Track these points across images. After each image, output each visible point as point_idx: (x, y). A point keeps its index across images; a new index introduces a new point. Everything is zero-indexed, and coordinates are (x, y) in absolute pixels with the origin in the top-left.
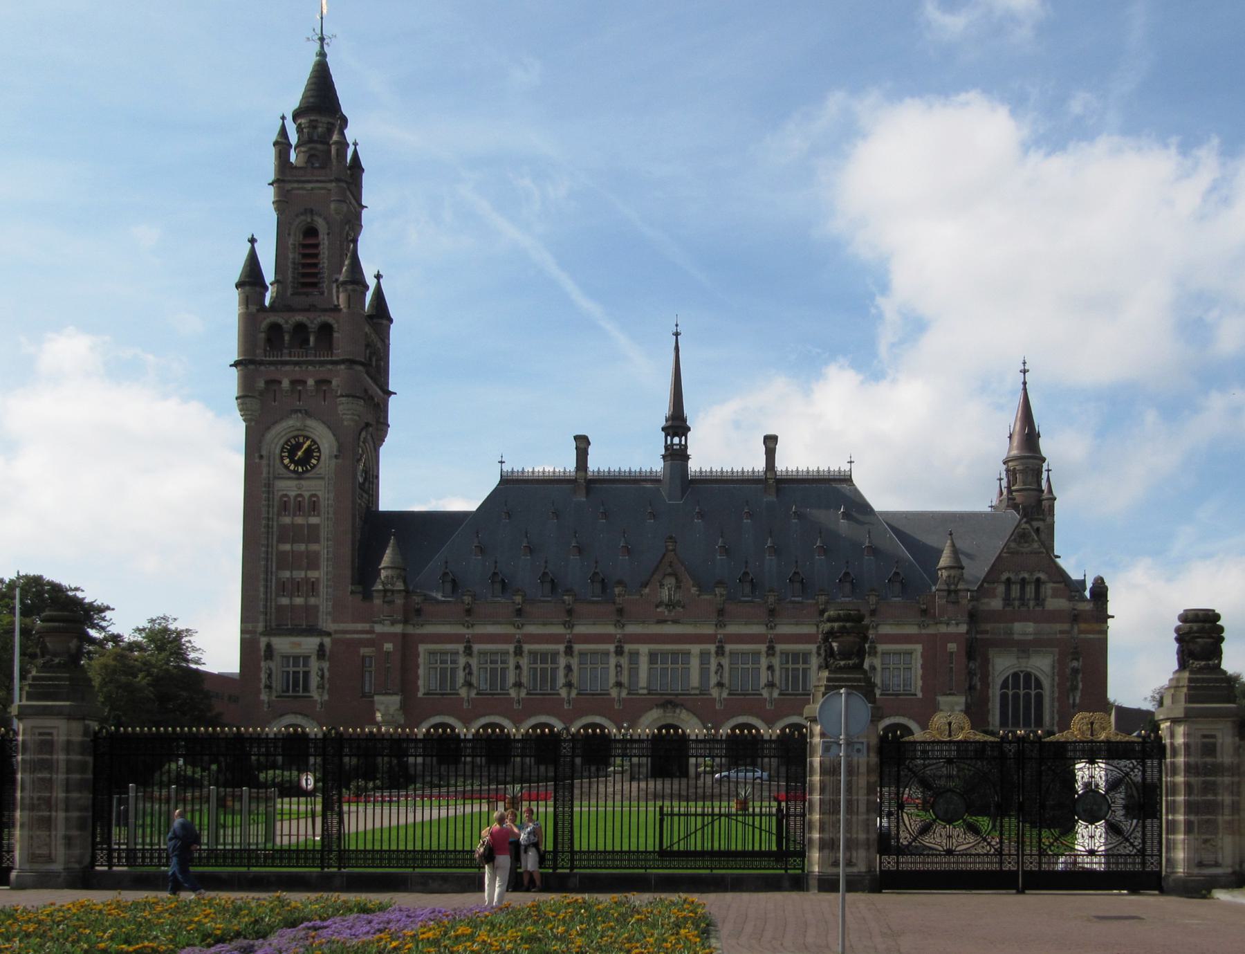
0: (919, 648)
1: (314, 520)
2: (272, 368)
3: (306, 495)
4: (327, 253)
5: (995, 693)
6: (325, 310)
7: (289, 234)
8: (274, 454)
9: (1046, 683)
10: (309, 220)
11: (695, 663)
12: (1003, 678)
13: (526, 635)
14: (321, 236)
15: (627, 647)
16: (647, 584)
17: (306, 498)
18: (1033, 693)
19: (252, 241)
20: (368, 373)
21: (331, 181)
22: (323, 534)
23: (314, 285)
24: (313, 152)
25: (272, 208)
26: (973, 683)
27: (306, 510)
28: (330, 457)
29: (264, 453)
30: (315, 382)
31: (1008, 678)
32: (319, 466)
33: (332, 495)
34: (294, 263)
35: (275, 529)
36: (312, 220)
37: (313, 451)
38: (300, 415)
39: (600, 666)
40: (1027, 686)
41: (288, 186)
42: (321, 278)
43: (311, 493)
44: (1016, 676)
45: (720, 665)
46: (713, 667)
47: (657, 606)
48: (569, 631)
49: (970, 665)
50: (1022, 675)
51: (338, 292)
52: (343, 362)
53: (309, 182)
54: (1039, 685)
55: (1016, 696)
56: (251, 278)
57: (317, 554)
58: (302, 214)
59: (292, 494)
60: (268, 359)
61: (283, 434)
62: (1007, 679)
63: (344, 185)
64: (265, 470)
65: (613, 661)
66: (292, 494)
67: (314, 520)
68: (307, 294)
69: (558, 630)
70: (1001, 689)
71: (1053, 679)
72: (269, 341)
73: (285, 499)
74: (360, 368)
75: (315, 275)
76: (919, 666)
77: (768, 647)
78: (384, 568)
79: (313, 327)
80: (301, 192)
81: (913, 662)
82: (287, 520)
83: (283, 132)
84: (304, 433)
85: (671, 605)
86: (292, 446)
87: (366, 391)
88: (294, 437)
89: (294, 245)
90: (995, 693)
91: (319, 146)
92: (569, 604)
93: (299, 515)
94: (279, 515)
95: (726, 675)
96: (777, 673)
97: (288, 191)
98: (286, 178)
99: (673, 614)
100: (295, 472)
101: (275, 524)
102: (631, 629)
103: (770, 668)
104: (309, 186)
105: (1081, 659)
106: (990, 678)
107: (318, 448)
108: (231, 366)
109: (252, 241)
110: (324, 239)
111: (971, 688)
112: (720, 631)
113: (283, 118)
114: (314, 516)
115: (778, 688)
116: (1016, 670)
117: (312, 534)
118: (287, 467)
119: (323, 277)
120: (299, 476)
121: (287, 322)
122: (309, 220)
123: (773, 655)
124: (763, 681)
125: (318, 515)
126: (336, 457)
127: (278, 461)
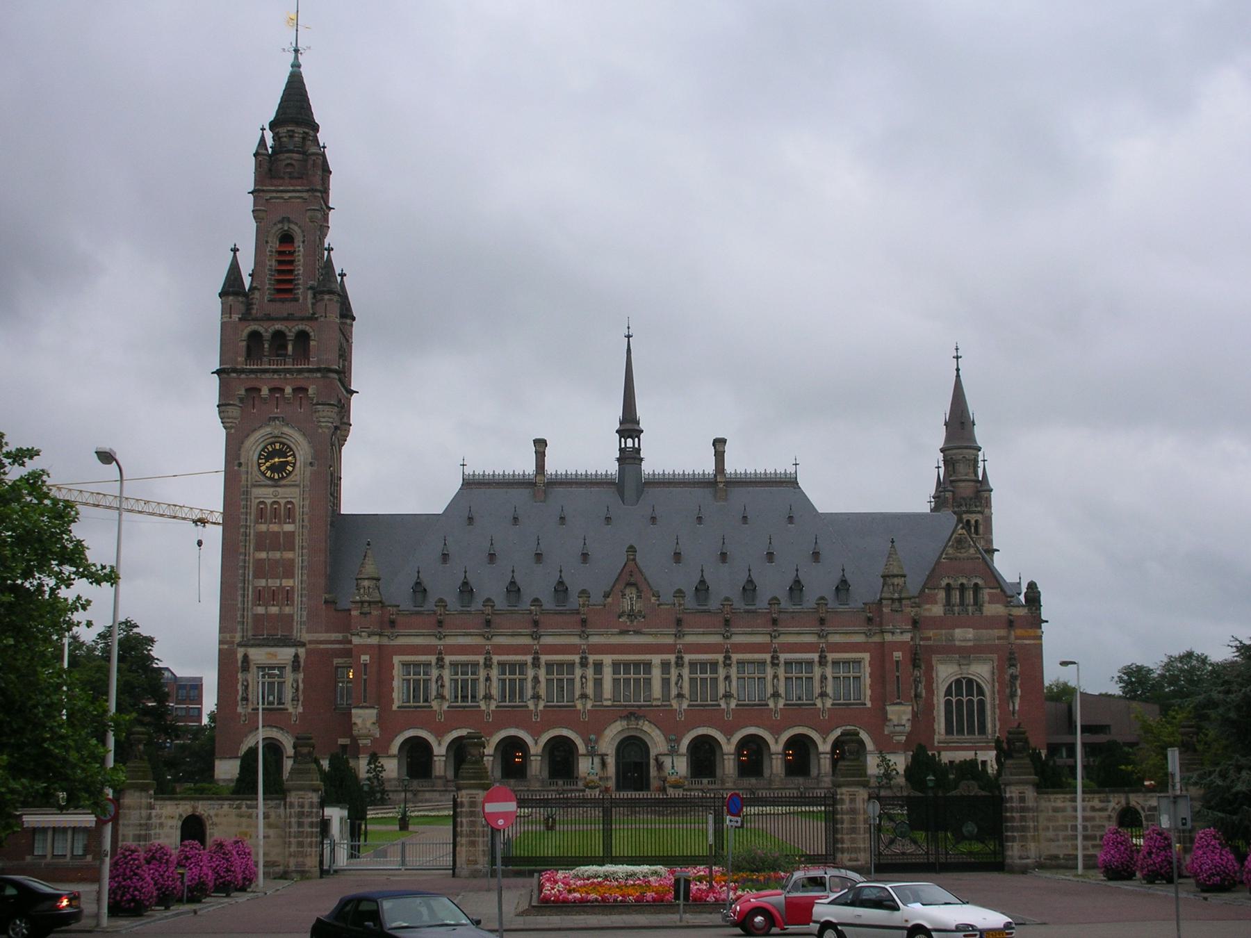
0: (866, 656)
1: (288, 528)
2: (253, 376)
3: (282, 501)
4: (301, 258)
6: (302, 319)
7: (267, 242)
8: (252, 459)
10: (286, 228)
11: (656, 673)
12: (947, 685)
13: (495, 646)
15: (591, 658)
16: (610, 594)
17: (282, 505)
18: (975, 699)
19: (235, 250)
20: (340, 380)
24: (289, 161)
26: (919, 690)
27: (283, 519)
29: (242, 461)
30: (293, 390)
31: (951, 684)
33: (307, 503)
34: (271, 270)
35: (252, 537)
38: (277, 422)
39: (565, 676)
40: (970, 693)
41: (268, 196)
42: (296, 285)
43: (286, 500)
44: (958, 682)
45: (680, 676)
46: (674, 679)
47: (620, 617)
48: (536, 642)
49: (915, 672)
52: (318, 370)
54: (981, 692)
55: (959, 703)
56: (232, 287)
57: (293, 560)
58: (279, 222)
59: (269, 501)
60: (248, 367)
61: (262, 440)
63: (319, 194)
65: (578, 672)
66: (269, 501)
67: (288, 528)
68: (283, 301)
69: (527, 641)
70: (945, 696)
71: (994, 686)
72: (248, 347)
73: (262, 506)
74: (335, 376)
75: (290, 281)
77: (725, 657)
79: (291, 335)
80: (278, 201)
81: (862, 670)
82: (263, 528)
83: (263, 140)
84: (281, 440)
85: (631, 615)
86: (269, 453)
88: (273, 443)
89: (271, 251)
91: (296, 156)
92: (536, 615)
93: (275, 523)
94: (257, 522)
95: (686, 685)
96: (734, 683)
97: (267, 200)
98: (265, 188)
99: (635, 623)
100: (271, 479)
101: (252, 531)
102: (594, 640)
103: (727, 678)
104: (287, 195)
105: (1019, 666)
106: (935, 685)
108: (213, 373)
109: (235, 250)
110: (300, 247)
113: (263, 129)
114: (289, 523)
115: (735, 698)
116: (959, 676)
117: (288, 542)
118: (264, 474)
119: (298, 284)
120: (276, 483)
121: (266, 331)
123: (730, 665)
124: (721, 691)
125: (294, 522)
126: (311, 463)
127: (256, 468)
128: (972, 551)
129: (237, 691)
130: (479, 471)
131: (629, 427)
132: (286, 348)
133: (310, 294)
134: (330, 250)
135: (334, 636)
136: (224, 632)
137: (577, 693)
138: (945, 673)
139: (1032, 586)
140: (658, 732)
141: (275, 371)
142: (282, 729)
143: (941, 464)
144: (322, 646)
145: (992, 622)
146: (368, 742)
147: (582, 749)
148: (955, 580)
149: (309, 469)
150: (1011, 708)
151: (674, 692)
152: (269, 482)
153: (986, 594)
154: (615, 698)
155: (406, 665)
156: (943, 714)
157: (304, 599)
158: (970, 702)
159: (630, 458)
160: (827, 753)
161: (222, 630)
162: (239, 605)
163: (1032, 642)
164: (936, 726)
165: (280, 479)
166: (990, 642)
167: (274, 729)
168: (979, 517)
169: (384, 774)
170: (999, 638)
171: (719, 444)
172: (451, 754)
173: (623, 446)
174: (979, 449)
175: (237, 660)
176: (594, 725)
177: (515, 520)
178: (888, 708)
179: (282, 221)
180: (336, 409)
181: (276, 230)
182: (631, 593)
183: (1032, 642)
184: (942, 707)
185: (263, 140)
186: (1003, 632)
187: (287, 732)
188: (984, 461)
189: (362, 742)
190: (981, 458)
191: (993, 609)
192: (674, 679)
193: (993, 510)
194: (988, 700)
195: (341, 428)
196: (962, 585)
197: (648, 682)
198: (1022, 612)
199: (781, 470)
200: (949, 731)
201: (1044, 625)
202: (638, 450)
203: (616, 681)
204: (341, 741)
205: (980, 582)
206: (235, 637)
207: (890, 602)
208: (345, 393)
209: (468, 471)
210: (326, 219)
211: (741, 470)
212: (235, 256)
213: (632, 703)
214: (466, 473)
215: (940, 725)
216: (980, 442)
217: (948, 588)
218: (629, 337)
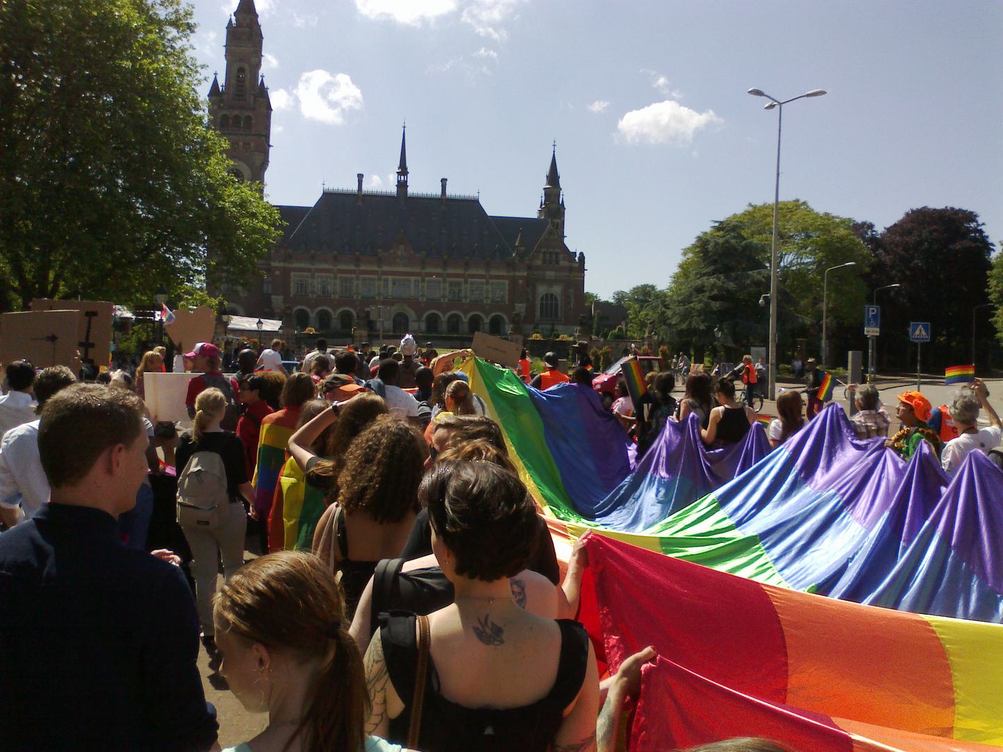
5: (538, 302)
9: (559, 298)
11: (412, 285)
12: (542, 295)
15: (384, 277)
18: (554, 302)
19: (216, 74)
25: (224, 58)
30: (244, 144)
40: (551, 300)
44: (547, 295)
54: (556, 299)
55: (547, 303)
62: (542, 298)
83: (230, 21)
90: (538, 302)
102: (385, 268)
104: (242, 48)
109: (216, 74)
110: (248, 75)
112: (424, 271)
131: (403, 170)
132: (240, 123)
133: (252, 98)
134: (262, 76)
137: (376, 292)
138: (542, 290)
139: (582, 254)
143: (543, 196)
146: (279, 311)
153: (561, 256)
155: (295, 276)
159: (402, 186)
168: (559, 221)
171: (444, 181)
178: (516, 305)
179: (240, 61)
180: (263, 154)
181: (236, 67)
182: (402, 247)
184: (539, 306)
185: (231, 19)
189: (276, 311)
190: (561, 194)
191: (563, 263)
192: (420, 287)
193: (565, 218)
194: (559, 303)
195: (265, 163)
196: (551, 253)
198: (577, 265)
199: (471, 195)
200: (541, 316)
201: (585, 272)
205: (558, 250)
211: (453, 194)
212: (216, 77)
215: (538, 313)
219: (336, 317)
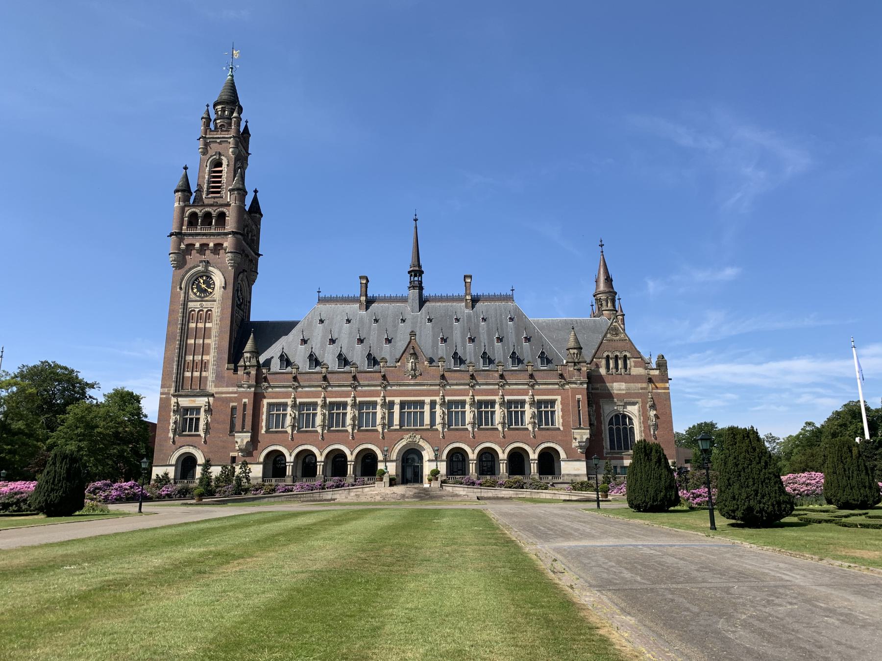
0: (559, 398)
1: (208, 325)
5: (605, 428)
11: (427, 408)
12: (610, 417)
14: (223, 166)
16: (399, 360)
19: (186, 168)
21: (230, 138)
22: (214, 333)
23: (219, 192)
28: (220, 287)
30: (214, 245)
31: (612, 418)
32: (213, 293)
33: (219, 310)
36: (219, 158)
37: (211, 284)
43: (206, 309)
44: (617, 416)
50: (620, 416)
51: (230, 196)
53: (219, 138)
55: (618, 429)
63: (237, 139)
64: (182, 295)
67: (208, 325)
68: (214, 198)
75: (219, 187)
76: (560, 410)
78: (245, 352)
79: (214, 214)
87: (244, 251)
90: (605, 428)
104: (218, 141)
106: (602, 418)
107: (214, 282)
109: (186, 168)
110: (224, 167)
111: (591, 425)
113: (208, 106)
116: (617, 413)
117: (206, 333)
118: (195, 294)
122: (218, 158)
128: (622, 336)
129: (170, 423)
130: (328, 295)
131: (416, 272)
135: (231, 389)
136: (164, 388)
140: (428, 445)
141: (204, 235)
142: (195, 447)
143: (594, 303)
144: (223, 395)
145: (636, 379)
147: (380, 457)
148: (612, 353)
149: (222, 289)
150: (652, 433)
151: (438, 420)
152: (198, 299)
154: (401, 424)
155: (269, 404)
156: (608, 436)
157: (214, 367)
158: (626, 428)
160: (535, 460)
161: (163, 386)
162: (175, 371)
163: (663, 391)
164: (604, 444)
165: (204, 297)
166: (636, 391)
167: (191, 447)
169: (250, 474)
170: (642, 389)
172: (300, 462)
173: (412, 280)
174: (616, 293)
175: (171, 405)
176: (386, 443)
177: (348, 321)
183: (663, 391)
186: (644, 385)
187: (199, 449)
188: (619, 299)
190: (617, 297)
192: (438, 410)
196: (616, 358)
197: (422, 413)
199: (503, 293)
200: (612, 448)
202: (421, 282)
203: (402, 414)
204: (232, 454)
205: (628, 355)
206: (170, 390)
207: (573, 364)
208: (254, 254)
209: (321, 295)
210: (246, 159)
213: (412, 427)
214: (321, 296)
215: (607, 443)
216: (615, 290)
217: (608, 358)
218: (416, 220)
219: (323, 459)
